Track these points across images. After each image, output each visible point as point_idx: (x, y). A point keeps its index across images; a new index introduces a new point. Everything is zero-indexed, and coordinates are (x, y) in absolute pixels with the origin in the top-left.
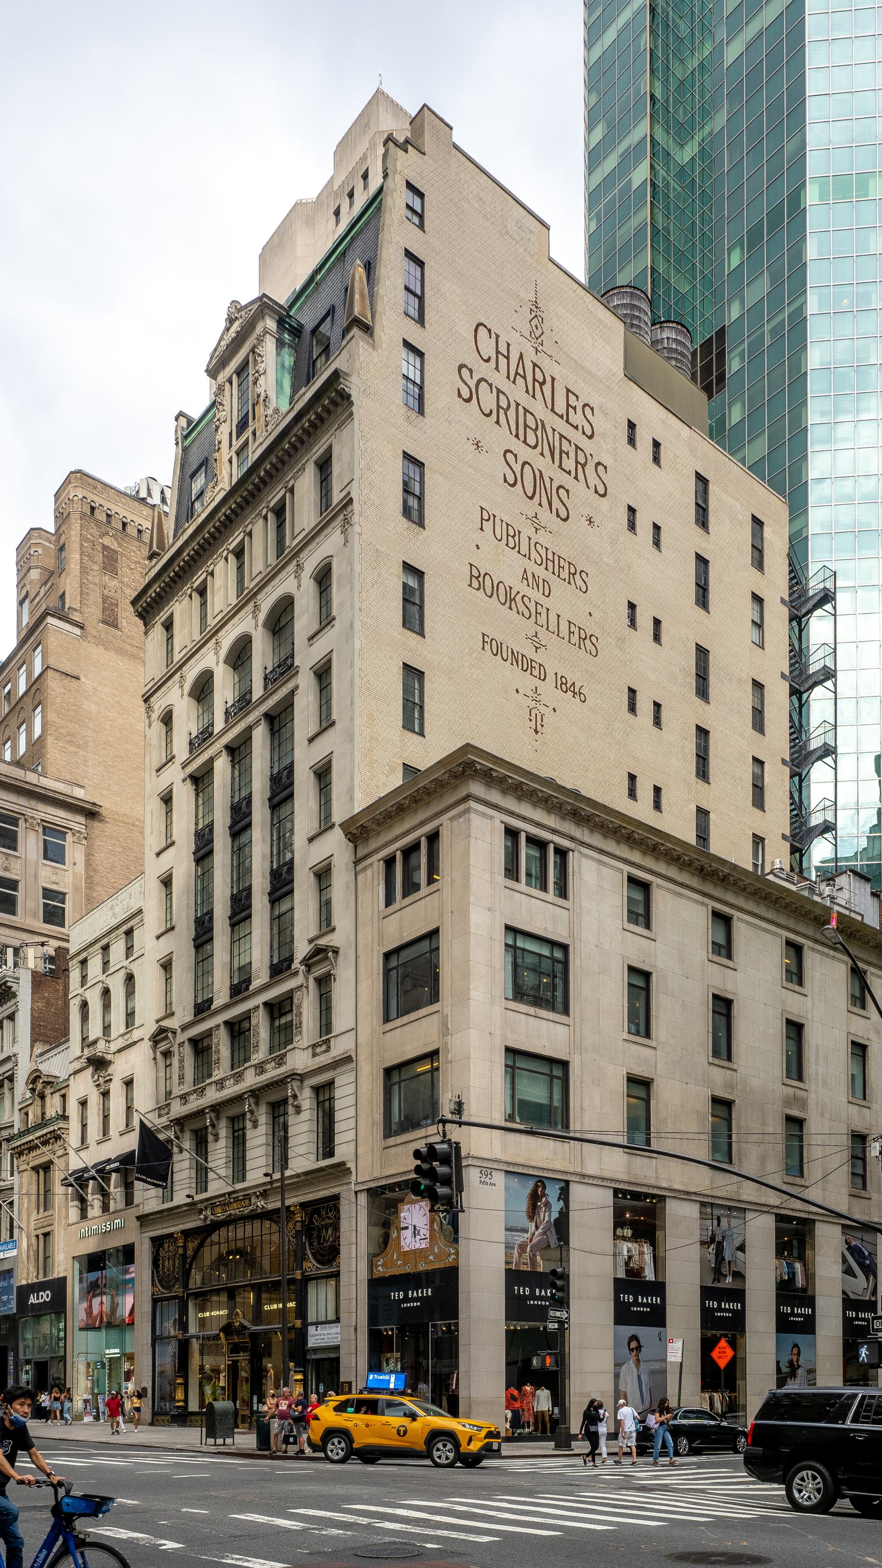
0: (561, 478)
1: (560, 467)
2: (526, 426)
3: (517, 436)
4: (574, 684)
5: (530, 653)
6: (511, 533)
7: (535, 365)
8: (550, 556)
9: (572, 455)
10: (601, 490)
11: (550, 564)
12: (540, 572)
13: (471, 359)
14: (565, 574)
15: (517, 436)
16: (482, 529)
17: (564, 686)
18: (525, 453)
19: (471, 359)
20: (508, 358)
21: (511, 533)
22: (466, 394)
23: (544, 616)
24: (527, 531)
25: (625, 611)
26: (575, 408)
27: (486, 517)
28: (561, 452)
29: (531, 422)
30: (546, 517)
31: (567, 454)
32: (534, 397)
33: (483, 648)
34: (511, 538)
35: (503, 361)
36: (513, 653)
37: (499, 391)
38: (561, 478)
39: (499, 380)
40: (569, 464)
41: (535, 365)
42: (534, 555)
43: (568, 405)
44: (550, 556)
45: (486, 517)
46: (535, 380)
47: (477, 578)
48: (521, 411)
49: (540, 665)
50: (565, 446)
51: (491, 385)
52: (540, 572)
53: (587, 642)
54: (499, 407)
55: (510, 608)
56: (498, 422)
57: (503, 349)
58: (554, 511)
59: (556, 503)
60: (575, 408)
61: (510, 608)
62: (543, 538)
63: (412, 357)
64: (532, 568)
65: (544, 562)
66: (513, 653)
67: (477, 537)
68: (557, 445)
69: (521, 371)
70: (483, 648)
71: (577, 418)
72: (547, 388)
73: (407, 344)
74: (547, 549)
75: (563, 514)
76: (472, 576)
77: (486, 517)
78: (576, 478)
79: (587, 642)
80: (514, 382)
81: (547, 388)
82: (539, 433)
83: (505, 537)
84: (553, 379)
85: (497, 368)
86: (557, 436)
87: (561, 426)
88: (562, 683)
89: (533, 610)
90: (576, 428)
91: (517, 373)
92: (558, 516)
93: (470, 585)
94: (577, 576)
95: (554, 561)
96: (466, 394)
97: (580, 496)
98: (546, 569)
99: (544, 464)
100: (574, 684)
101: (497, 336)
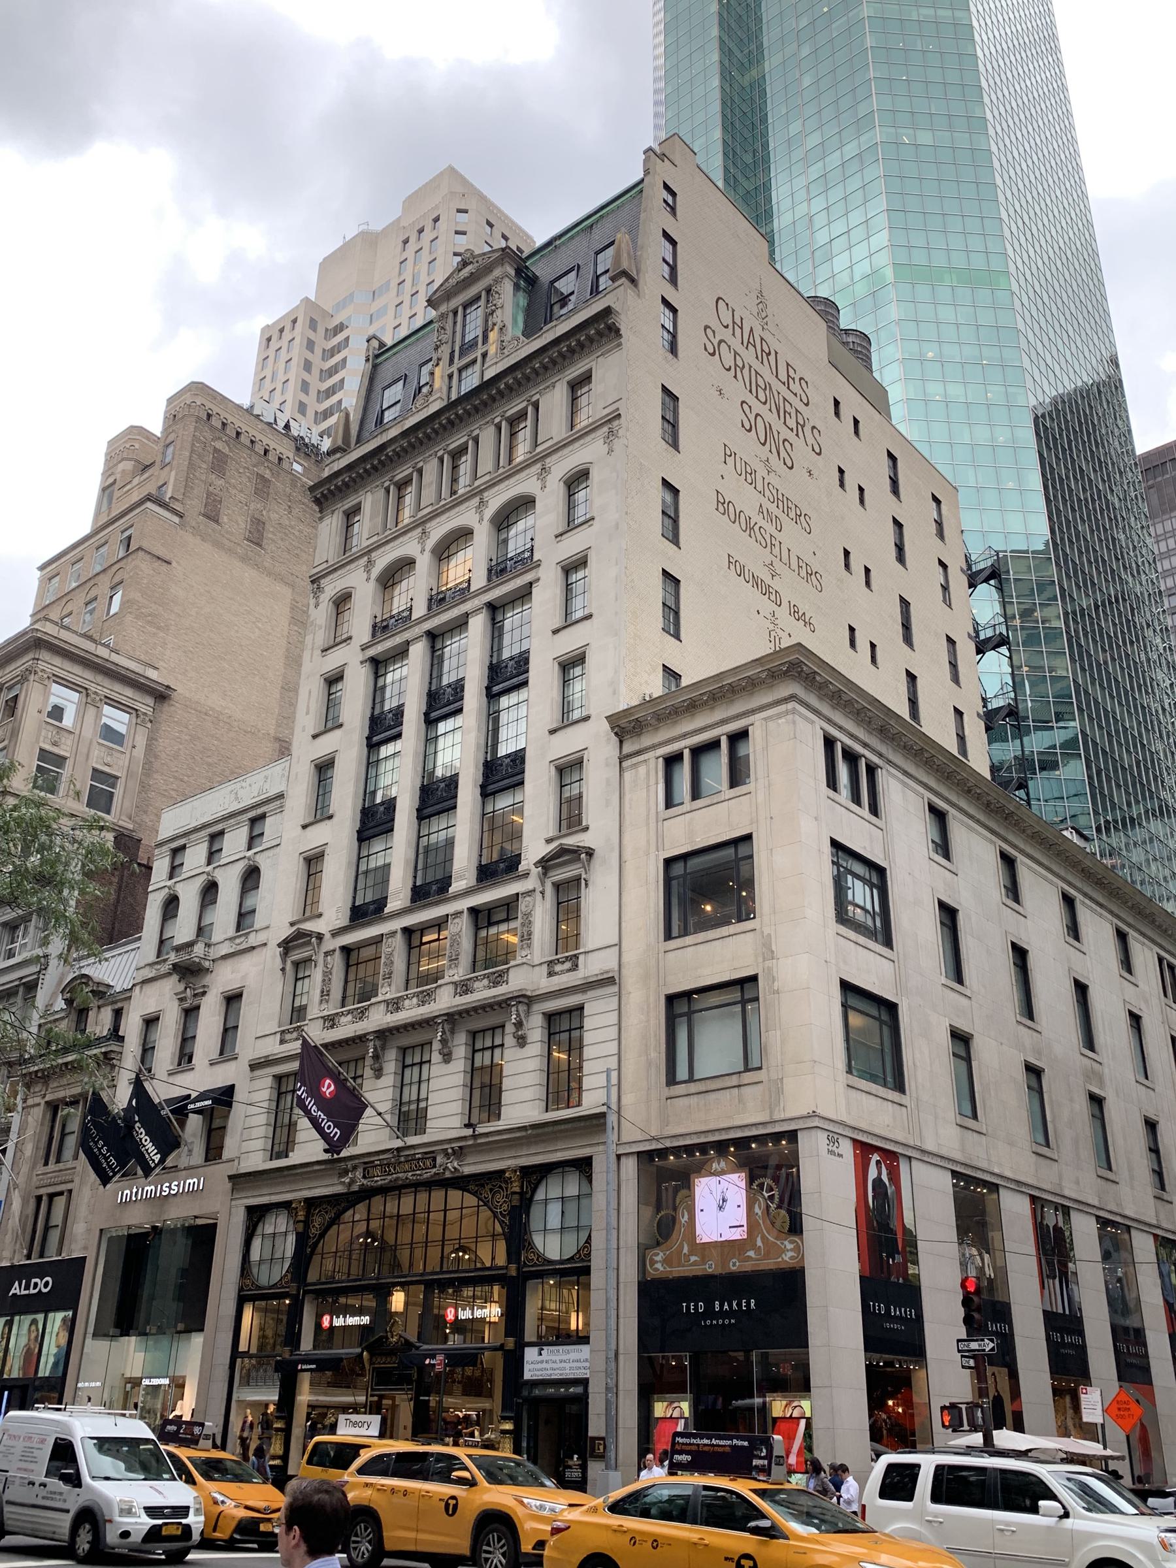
0: (786, 433)
2: (757, 385)
5: (768, 580)
8: (780, 497)
9: (793, 415)
11: (780, 503)
12: (772, 508)
15: (751, 391)
18: (758, 407)
24: (761, 472)
27: (729, 454)
35: (738, 330)
37: (736, 353)
38: (786, 433)
39: (735, 343)
40: (792, 423)
42: (767, 493)
44: (780, 497)
47: (723, 505)
57: (738, 321)
59: (783, 454)
62: (772, 479)
63: (667, 311)
64: (766, 504)
65: (776, 500)
71: (795, 387)
72: (772, 358)
73: (665, 301)
77: (729, 454)
81: (772, 358)
87: (783, 390)
97: (801, 451)
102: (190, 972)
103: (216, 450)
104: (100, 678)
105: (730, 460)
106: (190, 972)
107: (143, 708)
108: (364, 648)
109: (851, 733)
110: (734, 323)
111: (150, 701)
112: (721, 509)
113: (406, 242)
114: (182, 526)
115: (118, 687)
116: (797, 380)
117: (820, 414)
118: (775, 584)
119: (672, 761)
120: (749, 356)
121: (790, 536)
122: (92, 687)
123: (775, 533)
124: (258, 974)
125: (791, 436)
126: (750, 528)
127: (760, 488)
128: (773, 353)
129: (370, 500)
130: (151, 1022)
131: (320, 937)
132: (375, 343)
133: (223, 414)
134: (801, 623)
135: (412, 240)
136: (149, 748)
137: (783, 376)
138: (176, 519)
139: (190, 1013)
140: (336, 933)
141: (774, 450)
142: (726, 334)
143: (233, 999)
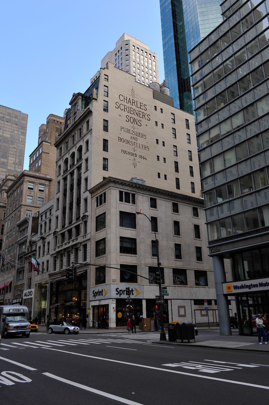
0: (139, 118)
5: (133, 152)
12: (135, 136)
13: (118, 100)
18: (130, 115)
19: (118, 100)
22: (117, 107)
27: (122, 128)
29: (132, 110)
34: (128, 131)
38: (139, 118)
39: (125, 103)
40: (141, 116)
47: (120, 139)
50: (140, 113)
52: (135, 136)
59: (138, 123)
62: (135, 130)
64: (133, 136)
67: (120, 132)
72: (136, 103)
73: (104, 100)
75: (140, 125)
77: (122, 128)
81: (136, 103)
87: (139, 109)
95: (139, 134)
96: (117, 107)
102: (43, 238)
103: (56, 128)
104: (37, 180)
105: (123, 130)
106: (43, 238)
107: (47, 184)
108: (62, 176)
109: (126, 189)
111: (48, 182)
112: (120, 140)
113: (116, 54)
114: (51, 145)
115: (41, 181)
117: (150, 110)
118: (135, 153)
119: (97, 198)
120: (129, 105)
121: (140, 141)
122: (36, 182)
123: (135, 141)
124: (51, 239)
125: (141, 119)
126: (128, 142)
127: (131, 132)
129: (63, 146)
130: (40, 247)
131: (58, 232)
132: (67, 110)
136: (49, 191)
137: (139, 106)
138: (49, 144)
139: (44, 246)
140: (60, 231)
142: (122, 102)
143: (49, 243)
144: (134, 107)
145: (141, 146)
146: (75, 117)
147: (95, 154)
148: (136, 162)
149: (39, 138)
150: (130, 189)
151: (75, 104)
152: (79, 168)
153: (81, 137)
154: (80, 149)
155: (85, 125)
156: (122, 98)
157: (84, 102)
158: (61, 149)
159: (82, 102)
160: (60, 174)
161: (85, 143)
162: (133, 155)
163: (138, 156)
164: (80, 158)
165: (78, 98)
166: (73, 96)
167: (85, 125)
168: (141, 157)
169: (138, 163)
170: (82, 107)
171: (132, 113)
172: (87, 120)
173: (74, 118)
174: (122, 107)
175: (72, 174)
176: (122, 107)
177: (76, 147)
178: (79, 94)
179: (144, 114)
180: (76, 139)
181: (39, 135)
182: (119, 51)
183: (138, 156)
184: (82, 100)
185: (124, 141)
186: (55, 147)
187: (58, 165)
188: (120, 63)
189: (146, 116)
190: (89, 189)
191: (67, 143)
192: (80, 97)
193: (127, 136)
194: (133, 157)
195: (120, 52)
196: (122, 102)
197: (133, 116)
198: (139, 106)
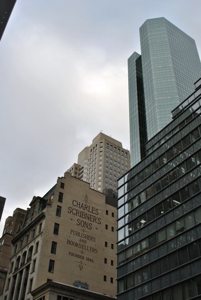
0: (90, 222)
1: (90, 220)
2: (83, 215)
3: (80, 217)
4: (91, 259)
5: (80, 254)
6: (78, 233)
7: (85, 205)
8: (87, 236)
9: (93, 218)
10: (99, 223)
11: (86, 238)
12: (84, 239)
13: (71, 205)
14: (90, 239)
16: (71, 233)
17: (88, 260)
18: (81, 219)
19: (71, 205)
20: (79, 205)
21: (78, 233)
23: (84, 247)
24: (81, 232)
25: (104, 244)
26: (94, 210)
28: (90, 218)
30: (86, 229)
31: (92, 218)
32: (85, 210)
33: (69, 255)
34: (78, 234)
36: (76, 255)
37: (77, 210)
38: (90, 222)
39: (78, 208)
41: (85, 205)
42: (83, 236)
43: (92, 210)
44: (87, 236)
45: (72, 231)
46: (85, 207)
47: (69, 242)
48: (82, 212)
49: (83, 256)
50: (91, 217)
51: (75, 210)
52: (84, 239)
53: (95, 251)
54: (77, 212)
55: (76, 246)
56: (76, 215)
58: (88, 228)
59: (89, 227)
60: (94, 210)
61: (76, 246)
62: (85, 233)
64: (82, 239)
66: (76, 255)
68: (89, 216)
69: (82, 206)
70: (69, 255)
71: (95, 212)
72: (88, 208)
74: (86, 235)
75: (90, 228)
76: (68, 241)
78: (94, 222)
79: (95, 251)
80: (81, 208)
81: (88, 208)
82: (85, 216)
83: (76, 234)
84: (89, 206)
85: (77, 207)
86: (90, 215)
87: (90, 214)
88: (88, 259)
89: (82, 247)
90: (94, 213)
91: (81, 207)
92: (89, 228)
93: (67, 244)
94: (93, 239)
95: (88, 237)
96: (70, 211)
97: (94, 225)
98: (86, 238)
99: (87, 221)
100: (91, 259)
101: (77, 202)
108: (13, 273)
110: (77, 204)
112: (68, 243)
113: (91, 150)
116: (95, 210)
120: (81, 210)
121: (89, 244)
125: (91, 222)
126: (76, 245)
128: (88, 207)
129: (18, 243)
133: (23, 213)
134: (90, 261)
135: (92, 150)
137: (91, 210)
141: (86, 227)
142: (75, 207)
144: (86, 211)
145: (89, 249)
146: (32, 218)
147: (40, 257)
148: (83, 265)
149: (4, 229)
150: (69, 294)
151: (34, 206)
152: (28, 268)
153: (34, 239)
154: (31, 249)
155: (38, 227)
156: (75, 203)
157: (42, 205)
158: (16, 246)
159: (40, 204)
160: (12, 271)
161: (35, 244)
162: (79, 257)
163: (85, 258)
164: (29, 259)
165: (37, 201)
166: (33, 199)
167: (38, 227)
168: (88, 259)
169: (84, 266)
170: (39, 209)
171: (84, 217)
172: (40, 223)
173: (32, 219)
174: (74, 212)
175: (21, 272)
176: (74, 212)
177: (35, 241)
178: (39, 198)
179: (95, 218)
180: (30, 239)
181: (5, 226)
182: (94, 148)
183: (85, 258)
184: (40, 203)
185: (73, 244)
186: (12, 243)
187: (12, 261)
188: (94, 158)
189: (97, 220)
190: (32, 290)
191: (22, 241)
192: (39, 200)
193: (76, 239)
194: (80, 260)
195: (95, 148)
196: (75, 207)
197: (84, 220)
198: (91, 210)
